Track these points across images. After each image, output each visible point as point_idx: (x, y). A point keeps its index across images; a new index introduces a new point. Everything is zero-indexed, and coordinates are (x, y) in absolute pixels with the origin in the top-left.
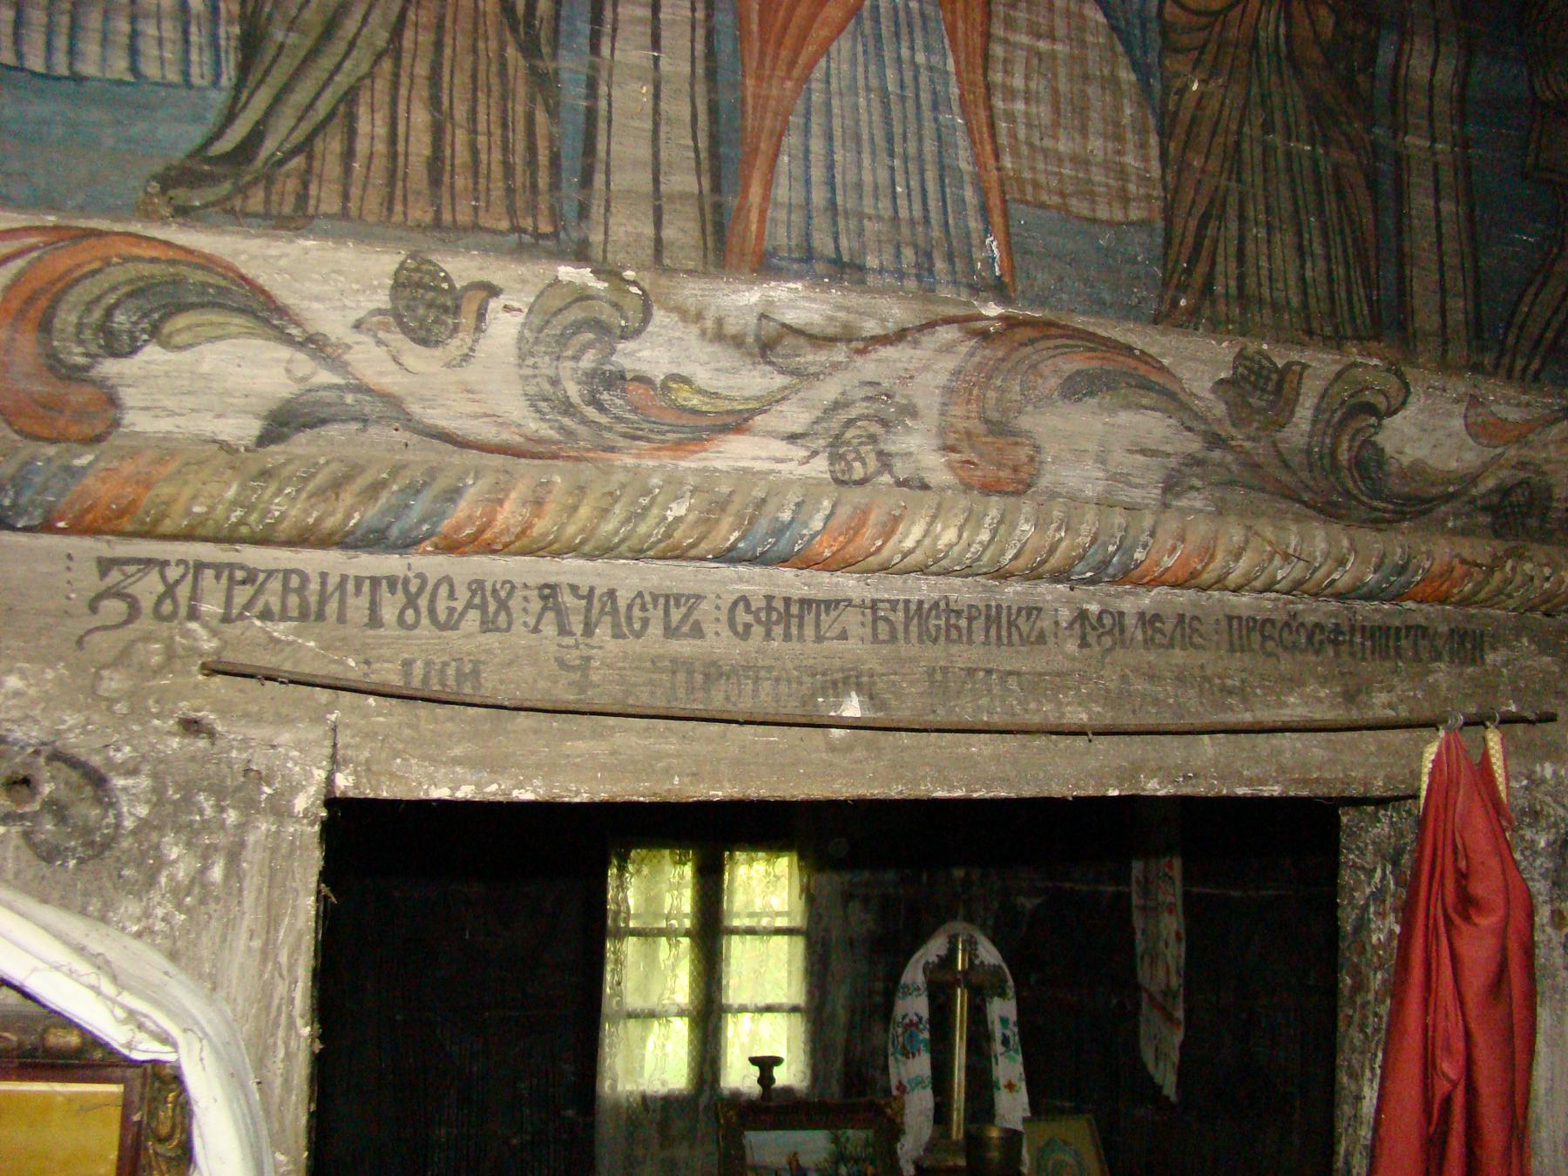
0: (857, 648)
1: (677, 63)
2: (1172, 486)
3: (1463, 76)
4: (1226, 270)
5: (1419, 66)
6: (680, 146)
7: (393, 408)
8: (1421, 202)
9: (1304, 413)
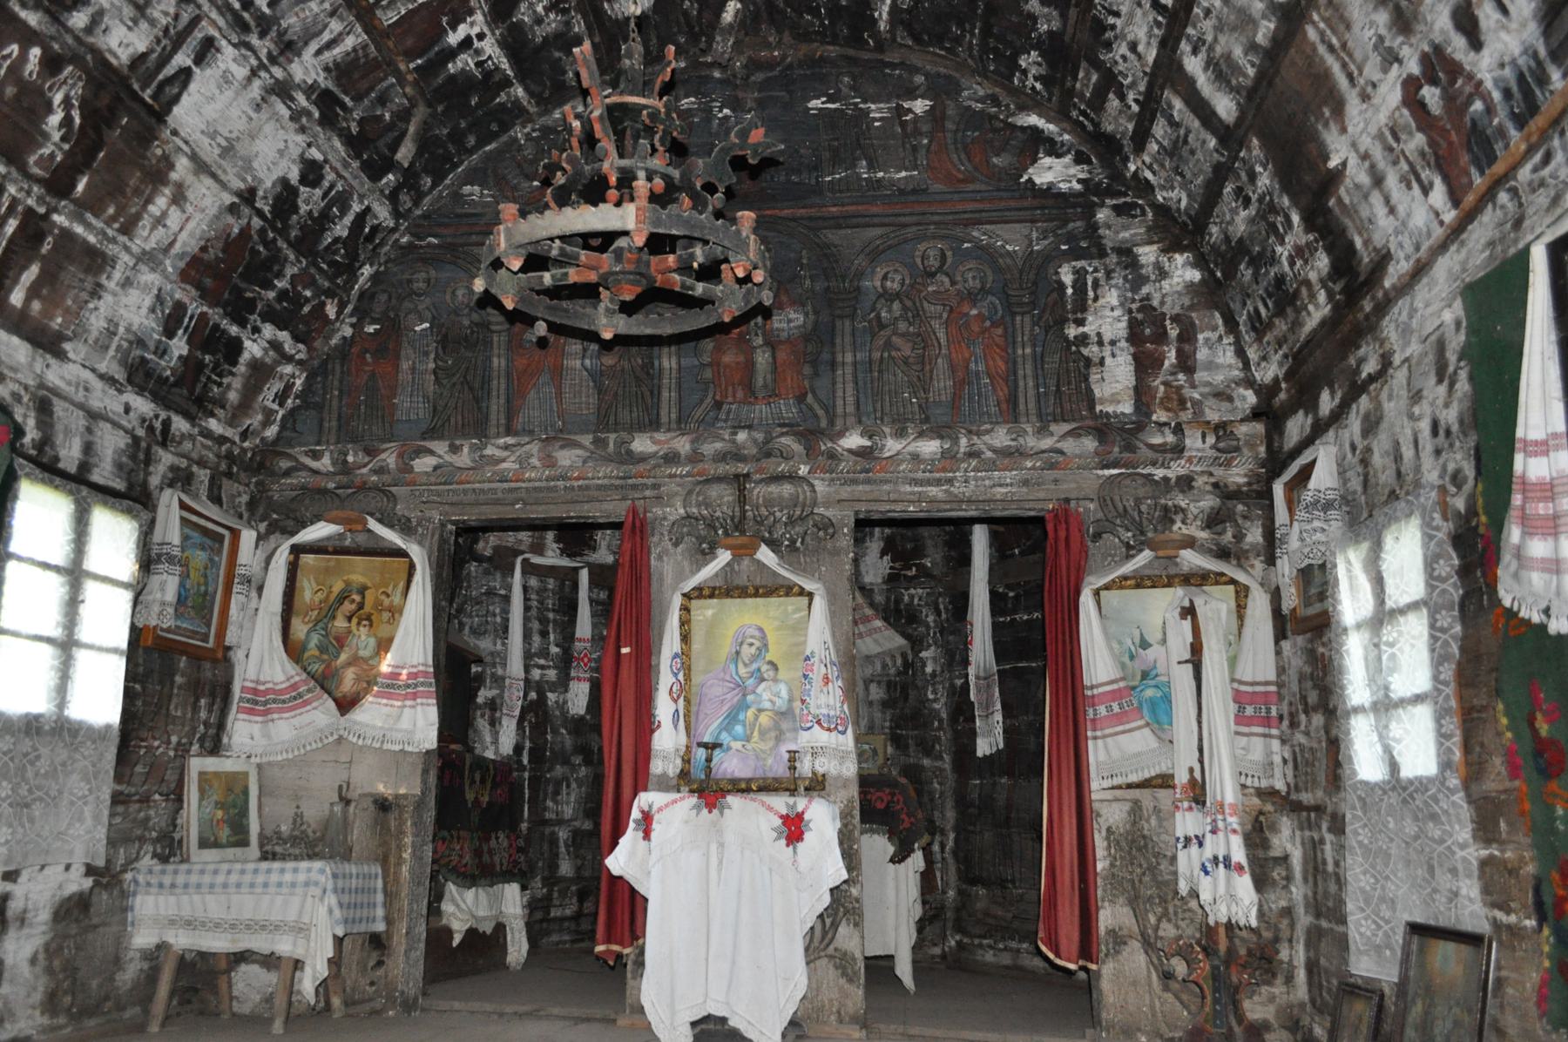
0: (523, 495)
1: (502, 401)
2: (584, 462)
3: (679, 364)
4: (612, 418)
5: (666, 364)
6: (502, 416)
7: (451, 464)
8: (665, 394)
9: (611, 445)
